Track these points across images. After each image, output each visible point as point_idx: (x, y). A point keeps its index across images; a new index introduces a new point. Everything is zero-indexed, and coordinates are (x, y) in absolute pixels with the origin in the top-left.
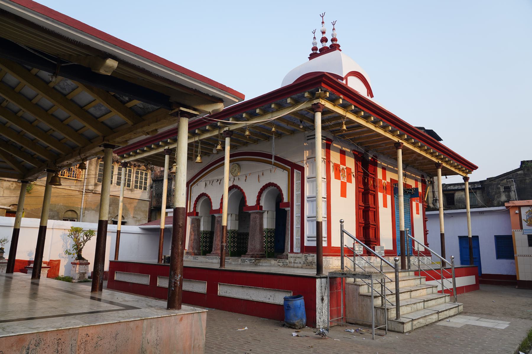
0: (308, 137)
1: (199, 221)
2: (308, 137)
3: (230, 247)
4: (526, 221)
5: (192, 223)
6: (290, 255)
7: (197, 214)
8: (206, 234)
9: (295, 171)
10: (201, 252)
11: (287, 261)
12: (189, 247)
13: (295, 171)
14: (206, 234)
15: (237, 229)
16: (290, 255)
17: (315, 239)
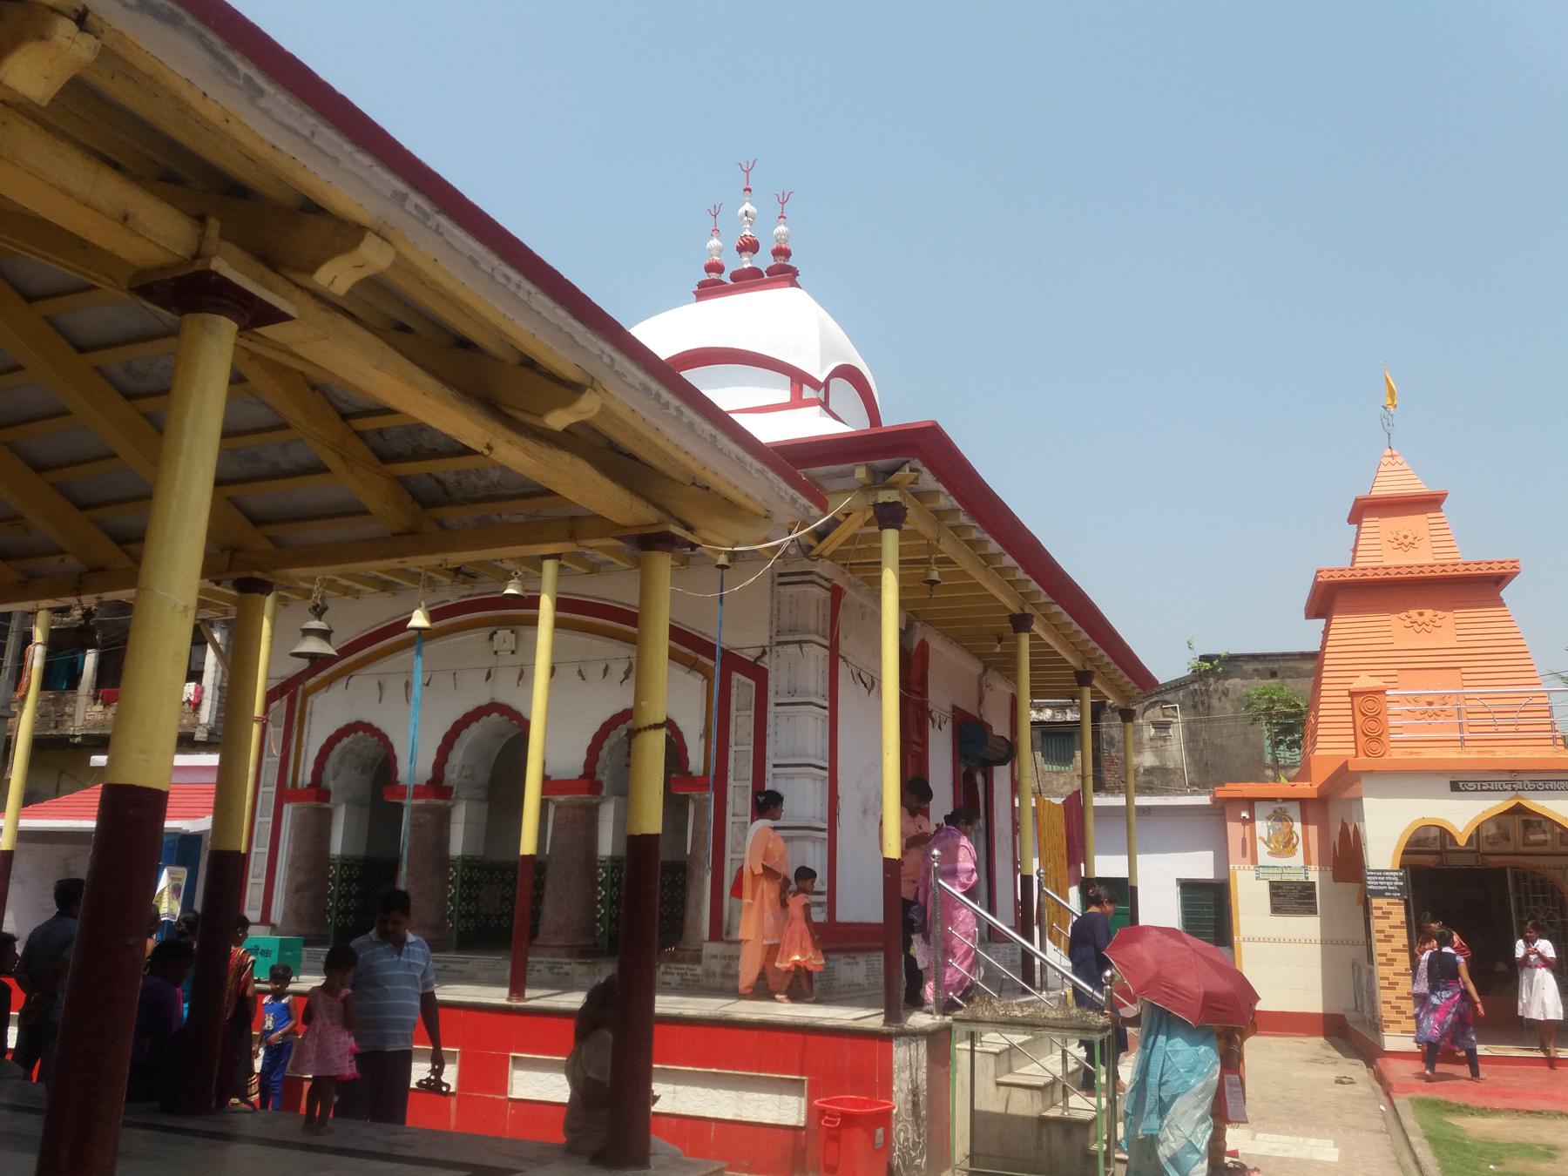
0: (781, 575)
1: (325, 818)
2: (781, 575)
3: (455, 917)
4: (1267, 843)
5: (300, 827)
6: (710, 948)
7: (324, 795)
8: (350, 867)
9: (736, 676)
10: (331, 932)
11: (699, 970)
12: (285, 915)
13: (736, 676)
14: (350, 867)
15: (479, 852)
16: (710, 948)
17: (824, 898)
